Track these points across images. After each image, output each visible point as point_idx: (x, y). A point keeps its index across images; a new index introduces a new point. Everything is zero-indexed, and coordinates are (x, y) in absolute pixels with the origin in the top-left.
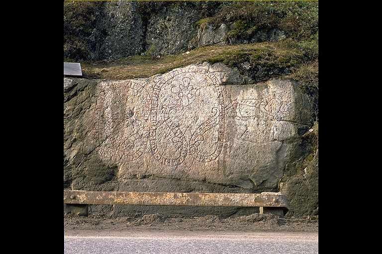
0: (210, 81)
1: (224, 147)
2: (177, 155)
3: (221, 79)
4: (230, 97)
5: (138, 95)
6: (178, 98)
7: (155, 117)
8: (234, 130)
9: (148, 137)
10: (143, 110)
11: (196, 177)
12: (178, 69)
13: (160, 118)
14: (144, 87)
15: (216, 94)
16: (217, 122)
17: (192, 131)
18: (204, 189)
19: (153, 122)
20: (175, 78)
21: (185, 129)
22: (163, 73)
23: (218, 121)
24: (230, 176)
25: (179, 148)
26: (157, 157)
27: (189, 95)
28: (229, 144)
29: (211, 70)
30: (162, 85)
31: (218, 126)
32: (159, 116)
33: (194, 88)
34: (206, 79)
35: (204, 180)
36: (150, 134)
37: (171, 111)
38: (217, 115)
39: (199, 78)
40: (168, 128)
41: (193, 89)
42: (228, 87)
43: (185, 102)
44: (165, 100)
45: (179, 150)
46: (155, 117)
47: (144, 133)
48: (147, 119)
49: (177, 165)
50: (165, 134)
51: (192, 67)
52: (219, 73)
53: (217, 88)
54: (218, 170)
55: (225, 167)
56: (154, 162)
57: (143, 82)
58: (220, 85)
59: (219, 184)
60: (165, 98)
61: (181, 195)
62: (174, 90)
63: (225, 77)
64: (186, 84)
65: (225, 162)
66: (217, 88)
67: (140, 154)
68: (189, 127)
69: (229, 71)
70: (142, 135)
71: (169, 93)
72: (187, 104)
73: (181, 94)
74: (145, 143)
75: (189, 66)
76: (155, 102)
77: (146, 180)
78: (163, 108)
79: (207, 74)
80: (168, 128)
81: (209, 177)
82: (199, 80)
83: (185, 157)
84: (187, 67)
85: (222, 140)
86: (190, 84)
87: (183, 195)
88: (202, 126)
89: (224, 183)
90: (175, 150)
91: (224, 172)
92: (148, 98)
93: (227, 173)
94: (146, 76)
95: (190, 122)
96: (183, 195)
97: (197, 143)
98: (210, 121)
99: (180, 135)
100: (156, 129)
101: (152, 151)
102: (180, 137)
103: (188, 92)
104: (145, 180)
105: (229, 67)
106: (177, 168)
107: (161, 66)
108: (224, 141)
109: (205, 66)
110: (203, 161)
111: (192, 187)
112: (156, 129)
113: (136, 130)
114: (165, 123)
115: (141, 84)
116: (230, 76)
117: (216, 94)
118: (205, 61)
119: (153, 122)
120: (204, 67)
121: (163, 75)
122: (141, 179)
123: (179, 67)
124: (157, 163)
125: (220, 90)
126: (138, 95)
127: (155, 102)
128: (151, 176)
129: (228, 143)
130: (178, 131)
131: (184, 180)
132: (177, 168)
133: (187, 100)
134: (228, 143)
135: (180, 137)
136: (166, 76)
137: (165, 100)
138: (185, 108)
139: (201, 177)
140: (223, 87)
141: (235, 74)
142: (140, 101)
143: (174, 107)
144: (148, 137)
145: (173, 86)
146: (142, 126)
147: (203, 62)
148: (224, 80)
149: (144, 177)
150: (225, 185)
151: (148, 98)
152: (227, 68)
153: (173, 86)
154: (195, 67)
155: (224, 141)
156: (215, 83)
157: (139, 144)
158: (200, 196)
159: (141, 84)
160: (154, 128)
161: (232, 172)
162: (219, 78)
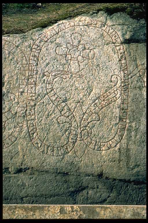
0: (108, 39)
1: (128, 130)
2: (63, 140)
3: (123, 35)
4: (135, 60)
5: (11, 57)
6: (65, 61)
7: (34, 88)
8: (141, 106)
9: (24, 117)
10: (17, 79)
11: (89, 170)
12: (64, 21)
13: (40, 91)
14: (18, 47)
15: (116, 56)
16: (118, 96)
17: (83, 107)
18: (100, 187)
19: (31, 95)
20: (60, 33)
21: (73, 105)
22: (44, 26)
23: (119, 93)
24: (136, 170)
25: (66, 131)
26: (37, 143)
27: (80, 58)
28: (134, 126)
29: (109, 23)
30: (42, 43)
31: (119, 101)
32: (39, 87)
33: (87, 47)
34: (102, 35)
35: (100, 175)
36: (27, 112)
37: (56, 80)
38: (119, 84)
39: (92, 33)
40: (52, 104)
41: (85, 49)
42: (133, 46)
43: (74, 67)
44: (48, 64)
45: (67, 133)
46: (34, 88)
47: (19, 110)
48: (23, 92)
49: (64, 155)
50: (46, 113)
51: (83, 18)
52: (120, 27)
53: (118, 48)
54: (120, 161)
55: (128, 157)
56: (33, 151)
57: (17, 40)
58: (122, 43)
59: (120, 180)
60: (47, 61)
61: (70, 209)
62: (60, 51)
63: (128, 33)
64: (76, 43)
65: (128, 150)
66: (118, 48)
67: (13, 139)
68: (80, 103)
69: (134, 24)
70: (16, 113)
71: (53, 55)
72: (76, 71)
73: (69, 57)
74: (21, 125)
75: (79, 17)
76: (33, 67)
77: (21, 175)
78: (44, 75)
79: (104, 28)
80: (52, 104)
81: (107, 171)
82: (94, 37)
83: (74, 143)
84: (76, 19)
85: (124, 120)
86: (82, 42)
87: (72, 208)
88: (97, 101)
89: (127, 178)
90: (60, 134)
91: (127, 164)
92: (24, 61)
93: (132, 165)
94: (22, 31)
95: (81, 95)
96: (72, 208)
97: (90, 125)
98: (109, 94)
99: (67, 114)
100: (35, 105)
101: (30, 136)
102: (68, 116)
103: (77, 53)
104: (20, 174)
105: (133, 18)
106: (63, 158)
107: (41, 17)
108: (128, 121)
109: (102, 17)
110: (99, 149)
111: (85, 184)
112: (35, 105)
113: (8, 107)
114: (47, 96)
115: (14, 43)
116: (135, 31)
117: (116, 56)
118: (101, 10)
119: (31, 95)
120: (99, 19)
121: (45, 30)
122: (15, 173)
123: (65, 19)
124: (37, 152)
125: (122, 51)
126: (11, 57)
127: (33, 67)
128: (29, 169)
129: (133, 124)
130: (65, 108)
131: (73, 175)
132: (63, 158)
133: (77, 64)
134: (133, 124)
135: (68, 116)
136: (48, 31)
137: (48, 64)
138: (74, 76)
139: (96, 170)
140: (125, 46)
141: (142, 27)
142: (13, 67)
143: (62, 73)
144: (24, 117)
145: (59, 45)
146: (16, 100)
147: (98, 11)
148: (127, 37)
149: (19, 171)
150: (129, 181)
151: (24, 61)
152: (131, 20)
153: (59, 45)
154: (88, 18)
155: (128, 121)
156: (114, 41)
157: (12, 125)
158: (98, 210)
159: (14, 43)
160: (32, 103)
161: (138, 163)
162: (119, 33)
